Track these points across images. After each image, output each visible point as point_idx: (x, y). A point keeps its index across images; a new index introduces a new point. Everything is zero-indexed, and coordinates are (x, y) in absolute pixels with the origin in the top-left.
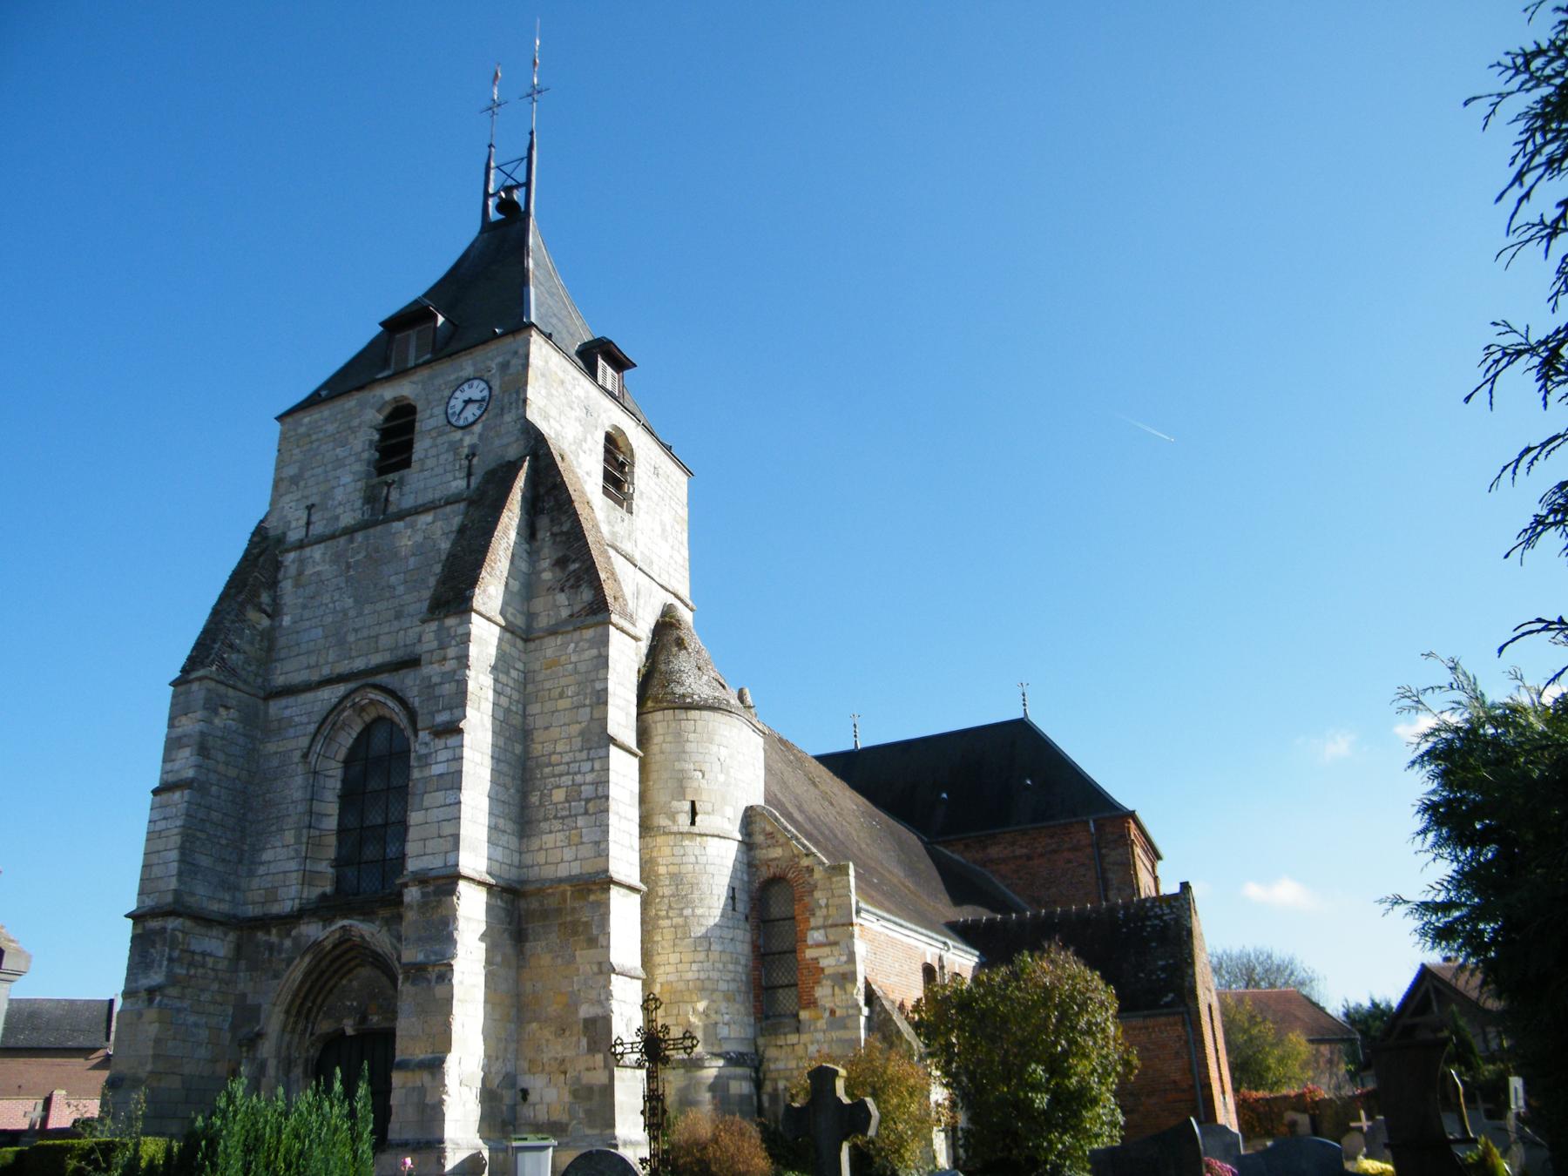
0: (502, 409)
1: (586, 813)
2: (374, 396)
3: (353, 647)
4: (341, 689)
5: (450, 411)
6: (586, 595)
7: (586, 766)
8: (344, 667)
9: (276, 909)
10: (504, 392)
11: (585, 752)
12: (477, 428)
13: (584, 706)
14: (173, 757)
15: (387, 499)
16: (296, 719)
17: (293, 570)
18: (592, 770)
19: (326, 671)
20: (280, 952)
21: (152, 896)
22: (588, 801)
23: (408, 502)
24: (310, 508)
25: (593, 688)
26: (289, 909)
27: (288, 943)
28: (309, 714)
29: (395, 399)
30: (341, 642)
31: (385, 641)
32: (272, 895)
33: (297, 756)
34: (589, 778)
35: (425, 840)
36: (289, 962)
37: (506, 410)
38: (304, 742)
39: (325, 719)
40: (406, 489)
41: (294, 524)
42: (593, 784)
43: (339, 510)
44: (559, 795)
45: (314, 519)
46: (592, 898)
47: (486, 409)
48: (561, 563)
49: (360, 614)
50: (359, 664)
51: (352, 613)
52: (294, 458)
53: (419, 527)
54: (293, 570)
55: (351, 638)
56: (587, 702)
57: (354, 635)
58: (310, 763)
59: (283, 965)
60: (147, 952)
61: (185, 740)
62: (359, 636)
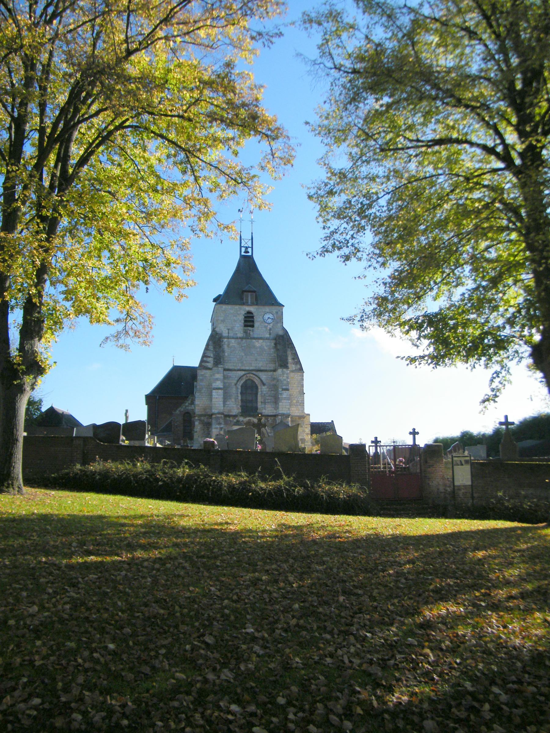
4: (243, 373)
6: (298, 366)
8: (243, 368)
9: (231, 414)
17: (226, 343)
19: (239, 368)
23: (256, 336)
24: (228, 329)
32: (230, 411)
38: (235, 382)
44: (295, 401)
48: (293, 359)
50: (247, 368)
54: (226, 343)
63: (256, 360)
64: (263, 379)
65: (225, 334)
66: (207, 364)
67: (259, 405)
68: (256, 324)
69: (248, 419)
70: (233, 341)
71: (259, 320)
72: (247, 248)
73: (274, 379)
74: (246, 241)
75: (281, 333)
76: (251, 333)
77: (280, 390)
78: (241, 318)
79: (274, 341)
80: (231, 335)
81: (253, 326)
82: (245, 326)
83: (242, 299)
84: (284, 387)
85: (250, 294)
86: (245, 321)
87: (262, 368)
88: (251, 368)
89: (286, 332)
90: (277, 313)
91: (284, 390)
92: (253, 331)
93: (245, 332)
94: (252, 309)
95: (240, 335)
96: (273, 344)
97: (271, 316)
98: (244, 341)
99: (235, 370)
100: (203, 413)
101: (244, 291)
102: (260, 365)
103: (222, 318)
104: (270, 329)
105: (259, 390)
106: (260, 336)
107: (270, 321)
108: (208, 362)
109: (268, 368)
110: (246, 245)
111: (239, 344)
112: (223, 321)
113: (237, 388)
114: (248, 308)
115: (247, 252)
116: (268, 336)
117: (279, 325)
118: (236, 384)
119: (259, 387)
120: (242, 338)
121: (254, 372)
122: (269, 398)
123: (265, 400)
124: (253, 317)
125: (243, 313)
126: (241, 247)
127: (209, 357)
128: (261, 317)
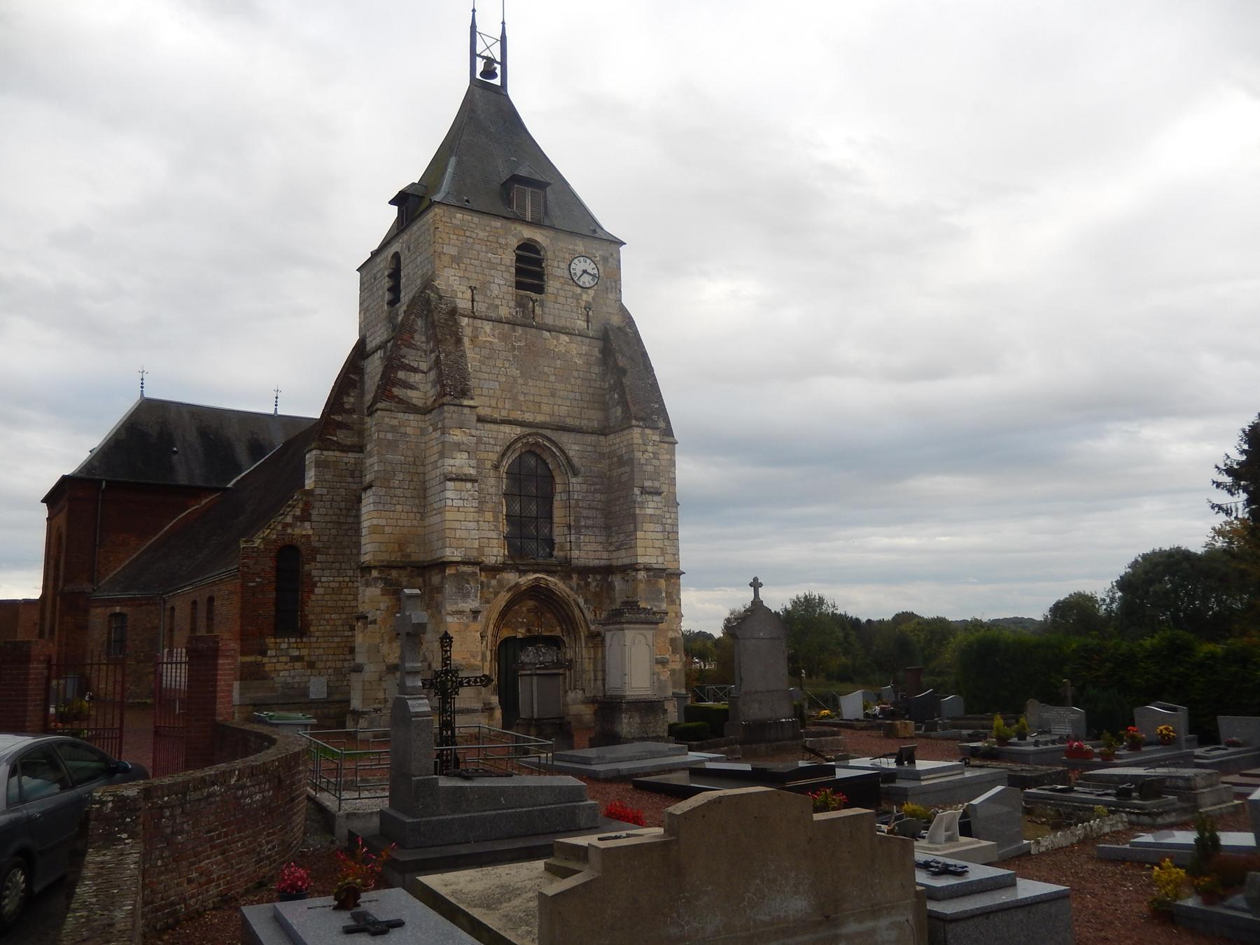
0: (607, 289)
1: (668, 538)
2: (515, 229)
3: (523, 404)
4: (518, 430)
5: (572, 271)
7: (667, 515)
8: (517, 415)
10: (607, 278)
11: (667, 508)
12: (591, 292)
13: (665, 484)
14: (454, 456)
15: (534, 311)
16: (485, 439)
18: (670, 518)
20: (488, 587)
21: (459, 550)
22: (669, 533)
23: (549, 320)
24: (472, 289)
25: (669, 475)
26: (494, 562)
27: (494, 582)
28: (496, 439)
29: (529, 239)
30: (514, 399)
31: (545, 408)
33: (488, 464)
34: (669, 521)
35: (646, 547)
36: (496, 594)
37: (609, 291)
38: (494, 457)
39: (509, 447)
40: (547, 310)
41: (460, 295)
42: (671, 525)
43: (498, 302)
45: (476, 298)
46: (672, 581)
47: (597, 283)
49: (526, 384)
50: (528, 417)
51: (520, 381)
52: (452, 241)
53: (561, 342)
55: (521, 398)
56: (666, 482)
57: (523, 396)
58: (500, 472)
59: (493, 595)
60: (463, 586)
61: (463, 447)
62: (527, 398)
63: (553, 395)
64: (571, 454)
65: (463, 304)
66: (410, 393)
67: (559, 535)
68: (552, 286)
69: (532, 576)
70: (488, 327)
71: (558, 272)
72: (490, 61)
73: (602, 455)
74: (489, 41)
75: (616, 320)
76: (538, 310)
77: (637, 491)
78: (509, 258)
79: (600, 343)
80: (481, 307)
81: (540, 289)
82: (519, 285)
83: (508, 202)
84: (647, 484)
85: (529, 190)
86: (519, 271)
87: (569, 421)
88: (540, 418)
89: (630, 321)
90: (605, 260)
91: (644, 491)
92: (542, 305)
93: (520, 304)
94: (538, 236)
95: (504, 312)
96: (596, 352)
97: (590, 267)
98: (520, 330)
99: (494, 422)
100: (396, 557)
101: (516, 179)
102: (563, 410)
103: (453, 251)
104: (588, 307)
105: (559, 488)
106: (561, 323)
107: (586, 280)
108: (411, 387)
109: (584, 423)
110: (485, 54)
111: (504, 338)
112: (456, 260)
113: (500, 478)
114: (528, 233)
115: (488, 73)
116: (581, 324)
117: (611, 296)
118: (496, 467)
119: (558, 480)
120: (513, 323)
121: (548, 433)
122: (591, 513)
123: (577, 520)
124: (539, 262)
125: (515, 243)
126: (473, 55)
127: (415, 370)
128: (564, 265)
